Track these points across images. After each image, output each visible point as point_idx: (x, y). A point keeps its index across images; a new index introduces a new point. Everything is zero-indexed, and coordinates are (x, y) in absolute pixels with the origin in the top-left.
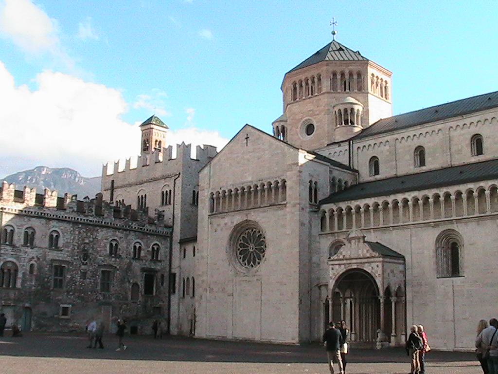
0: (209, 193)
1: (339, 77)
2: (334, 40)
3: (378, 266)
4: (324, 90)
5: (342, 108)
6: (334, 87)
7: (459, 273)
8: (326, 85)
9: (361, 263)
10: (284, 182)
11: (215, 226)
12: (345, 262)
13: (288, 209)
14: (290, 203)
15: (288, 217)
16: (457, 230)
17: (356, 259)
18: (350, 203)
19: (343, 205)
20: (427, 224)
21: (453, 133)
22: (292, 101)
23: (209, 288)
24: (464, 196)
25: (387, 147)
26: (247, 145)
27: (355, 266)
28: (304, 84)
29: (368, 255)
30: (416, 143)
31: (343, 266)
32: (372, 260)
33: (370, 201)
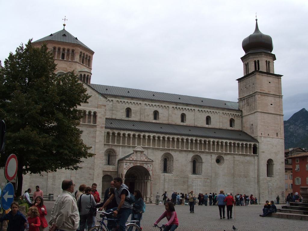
1: (82, 55)
2: (64, 29)
3: (151, 166)
5: (87, 74)
6: (80, 61)
7: (166, 171)
8: (77, 58)
9: (142, 163)
10: (95, 113)
12: (133, 162)
13: (98, 129)
14: (99, 125)
15: (98, 133)
16: (171, 153)
17: (140, 161)
19: (116, 132)
20: (158, 149)
21: (146, 107)
24: (176, 140)
25: (111, 103)
27: (139, 165)
28: (61, 50)
29: (146, 160)
30: (127, 106)
31: (132, 164)
32: (148, 163)
33: (132, 133)
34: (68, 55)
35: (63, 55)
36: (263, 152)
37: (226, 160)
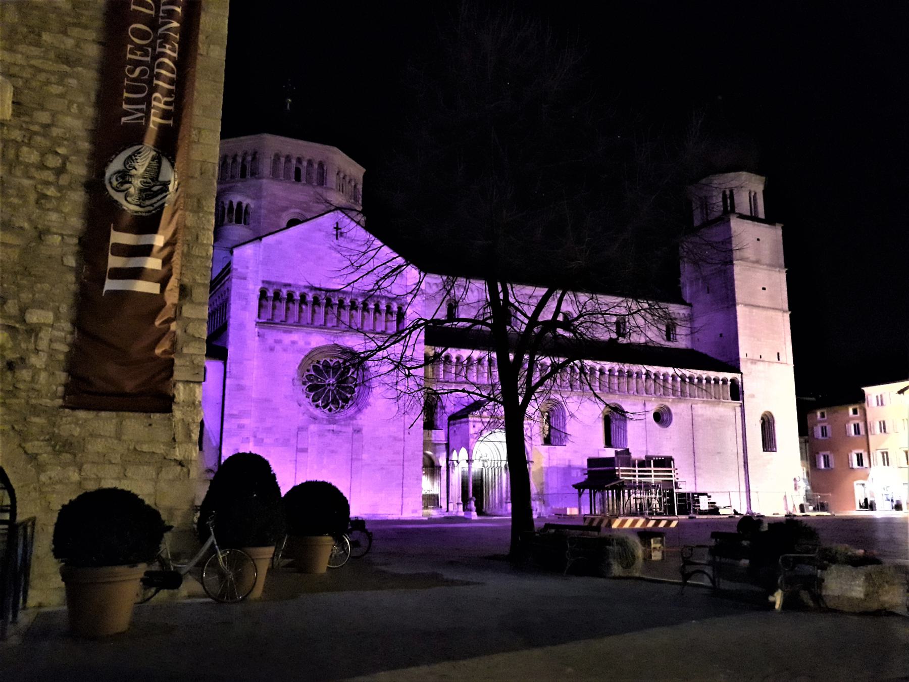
0: (259, 287)
4: (329, 185)
11: (270, 341)
18: (451, 351)
22: (271, 176)
23: (255, 437)
26: (337, 239)
28: (294, 161)
34: (308, 173)
35: (298, 171)
36: (753, 396)
37: (676, 414)
